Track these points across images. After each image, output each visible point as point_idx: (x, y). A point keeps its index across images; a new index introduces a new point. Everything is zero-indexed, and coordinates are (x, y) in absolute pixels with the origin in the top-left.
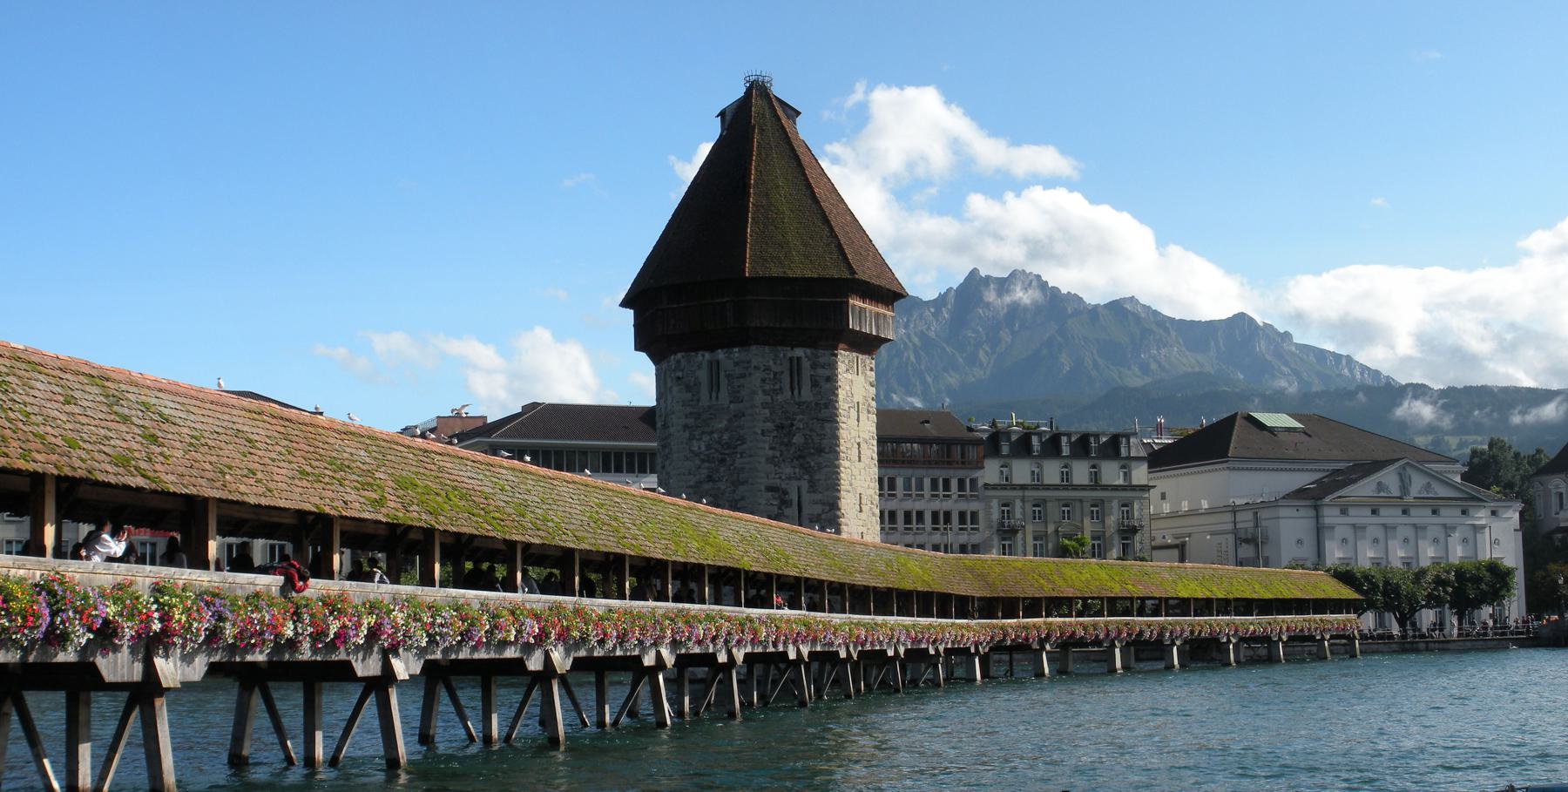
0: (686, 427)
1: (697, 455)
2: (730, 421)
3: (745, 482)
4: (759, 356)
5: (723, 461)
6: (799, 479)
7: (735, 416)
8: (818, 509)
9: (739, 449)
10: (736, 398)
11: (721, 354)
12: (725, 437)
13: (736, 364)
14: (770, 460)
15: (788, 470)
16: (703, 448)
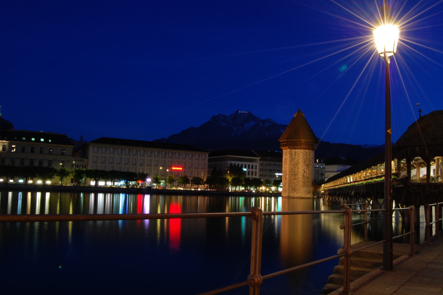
0: (290, 160)
1: (292, 164)
2: (297, 160)
3: (299, 169)
4: (302, 151)
5: (296, 166)
6: (307, 169)
7: (298, 159)
8: (309, 173)
9: (299, 164)
10: (298, 156)
11: (296, 150)
12: (297, 162)
13: (299, 152)
14: (303, 166)
15: (305, 167)
16: (293, 164)
